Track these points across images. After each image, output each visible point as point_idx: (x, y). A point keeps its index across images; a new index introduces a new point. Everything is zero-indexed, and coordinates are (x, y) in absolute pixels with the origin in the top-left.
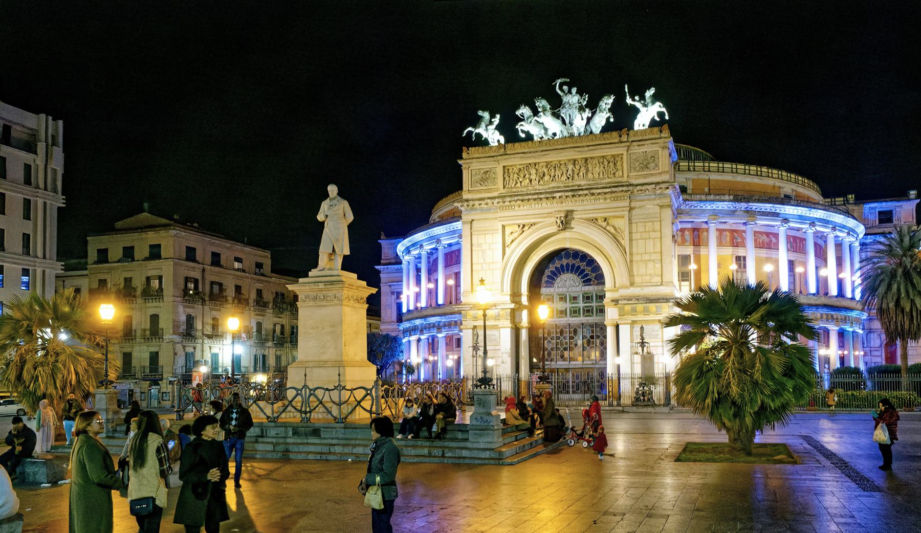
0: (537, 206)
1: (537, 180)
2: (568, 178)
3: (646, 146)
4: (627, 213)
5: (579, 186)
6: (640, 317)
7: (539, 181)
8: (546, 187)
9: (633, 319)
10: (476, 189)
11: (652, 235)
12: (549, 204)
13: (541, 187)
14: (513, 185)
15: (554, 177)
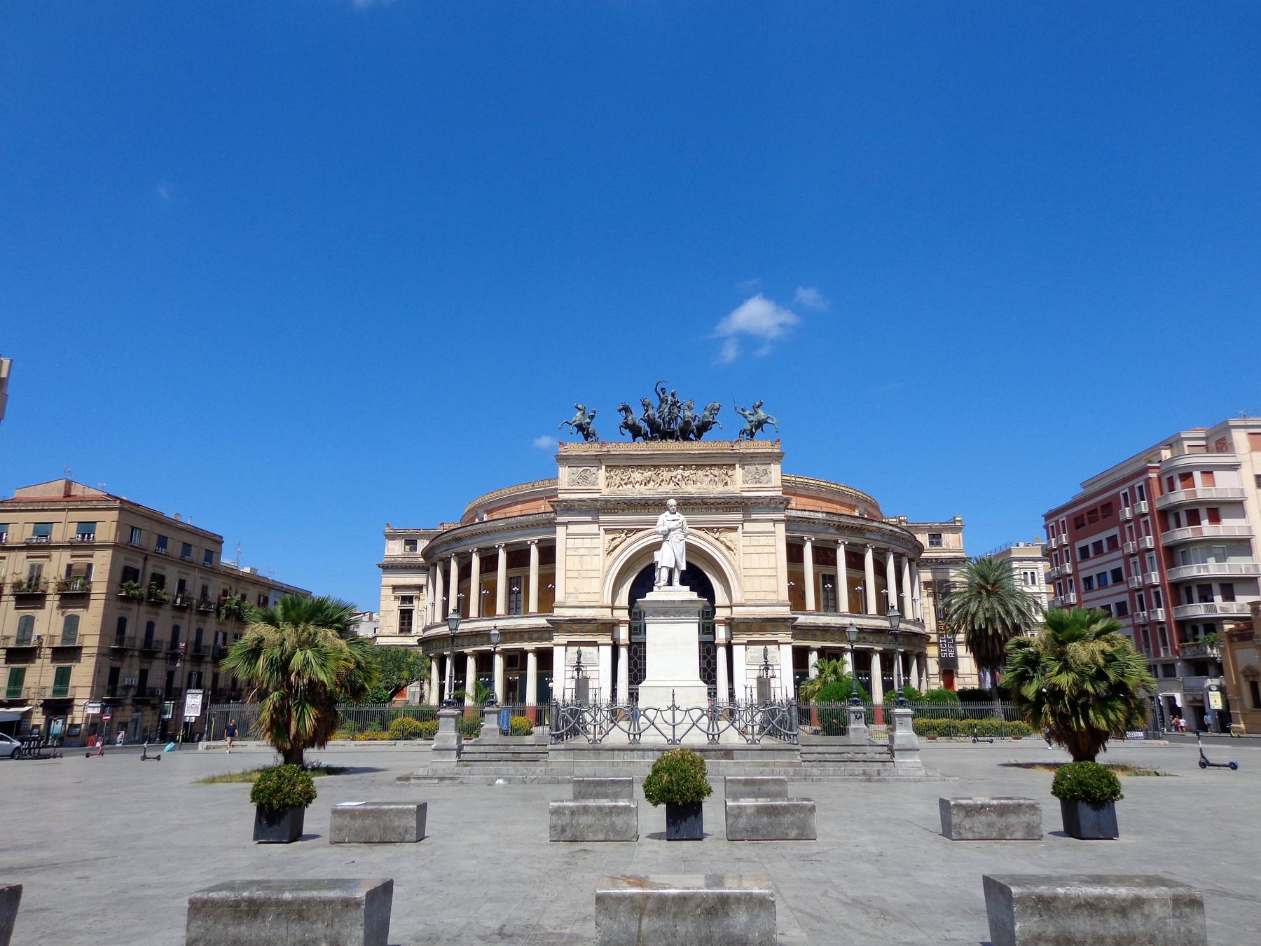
0: (643, 511)
1: (643, 484)
2: (678, 484)
3: (758, 459)
4: (740, 526)
5: (690, 493)
6: (756, 637)
7: (645, 485)
8: (652, 492)
9: (748, 639)
10: (573, 487)
11: (766, 550)
12: (656, 510)
13: (648, 492)
14: (616, 487)
15: (662, 481)
